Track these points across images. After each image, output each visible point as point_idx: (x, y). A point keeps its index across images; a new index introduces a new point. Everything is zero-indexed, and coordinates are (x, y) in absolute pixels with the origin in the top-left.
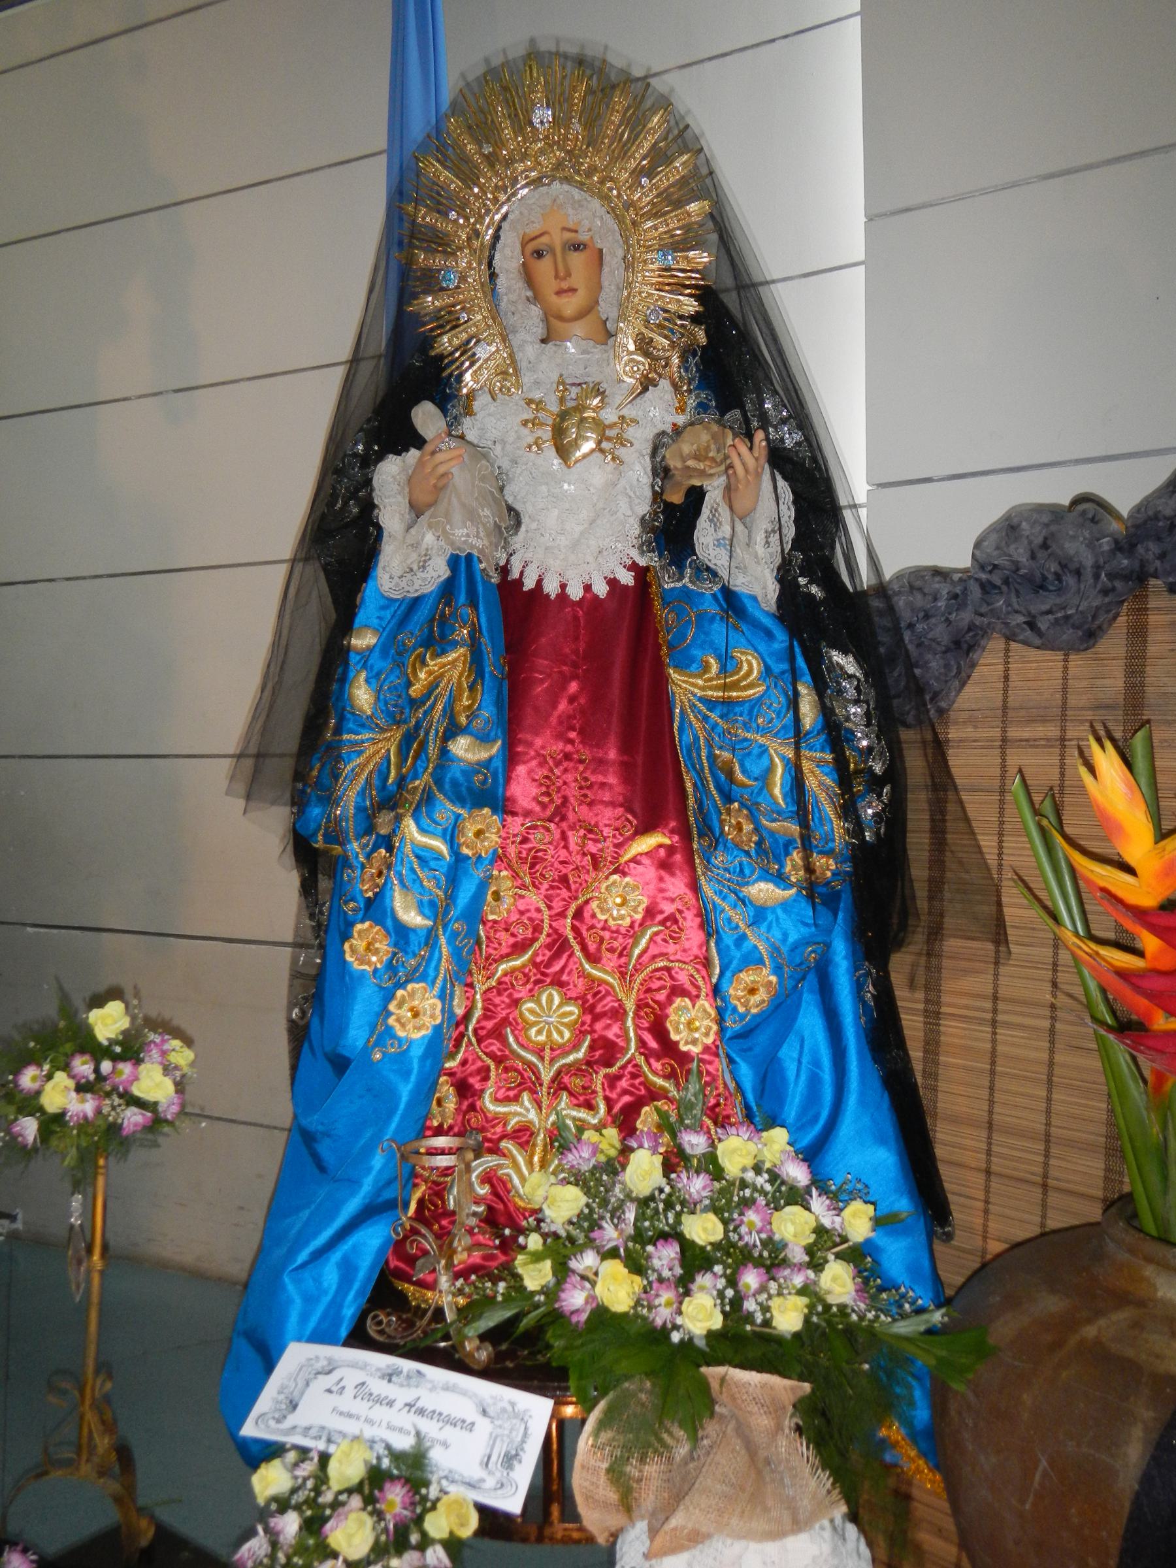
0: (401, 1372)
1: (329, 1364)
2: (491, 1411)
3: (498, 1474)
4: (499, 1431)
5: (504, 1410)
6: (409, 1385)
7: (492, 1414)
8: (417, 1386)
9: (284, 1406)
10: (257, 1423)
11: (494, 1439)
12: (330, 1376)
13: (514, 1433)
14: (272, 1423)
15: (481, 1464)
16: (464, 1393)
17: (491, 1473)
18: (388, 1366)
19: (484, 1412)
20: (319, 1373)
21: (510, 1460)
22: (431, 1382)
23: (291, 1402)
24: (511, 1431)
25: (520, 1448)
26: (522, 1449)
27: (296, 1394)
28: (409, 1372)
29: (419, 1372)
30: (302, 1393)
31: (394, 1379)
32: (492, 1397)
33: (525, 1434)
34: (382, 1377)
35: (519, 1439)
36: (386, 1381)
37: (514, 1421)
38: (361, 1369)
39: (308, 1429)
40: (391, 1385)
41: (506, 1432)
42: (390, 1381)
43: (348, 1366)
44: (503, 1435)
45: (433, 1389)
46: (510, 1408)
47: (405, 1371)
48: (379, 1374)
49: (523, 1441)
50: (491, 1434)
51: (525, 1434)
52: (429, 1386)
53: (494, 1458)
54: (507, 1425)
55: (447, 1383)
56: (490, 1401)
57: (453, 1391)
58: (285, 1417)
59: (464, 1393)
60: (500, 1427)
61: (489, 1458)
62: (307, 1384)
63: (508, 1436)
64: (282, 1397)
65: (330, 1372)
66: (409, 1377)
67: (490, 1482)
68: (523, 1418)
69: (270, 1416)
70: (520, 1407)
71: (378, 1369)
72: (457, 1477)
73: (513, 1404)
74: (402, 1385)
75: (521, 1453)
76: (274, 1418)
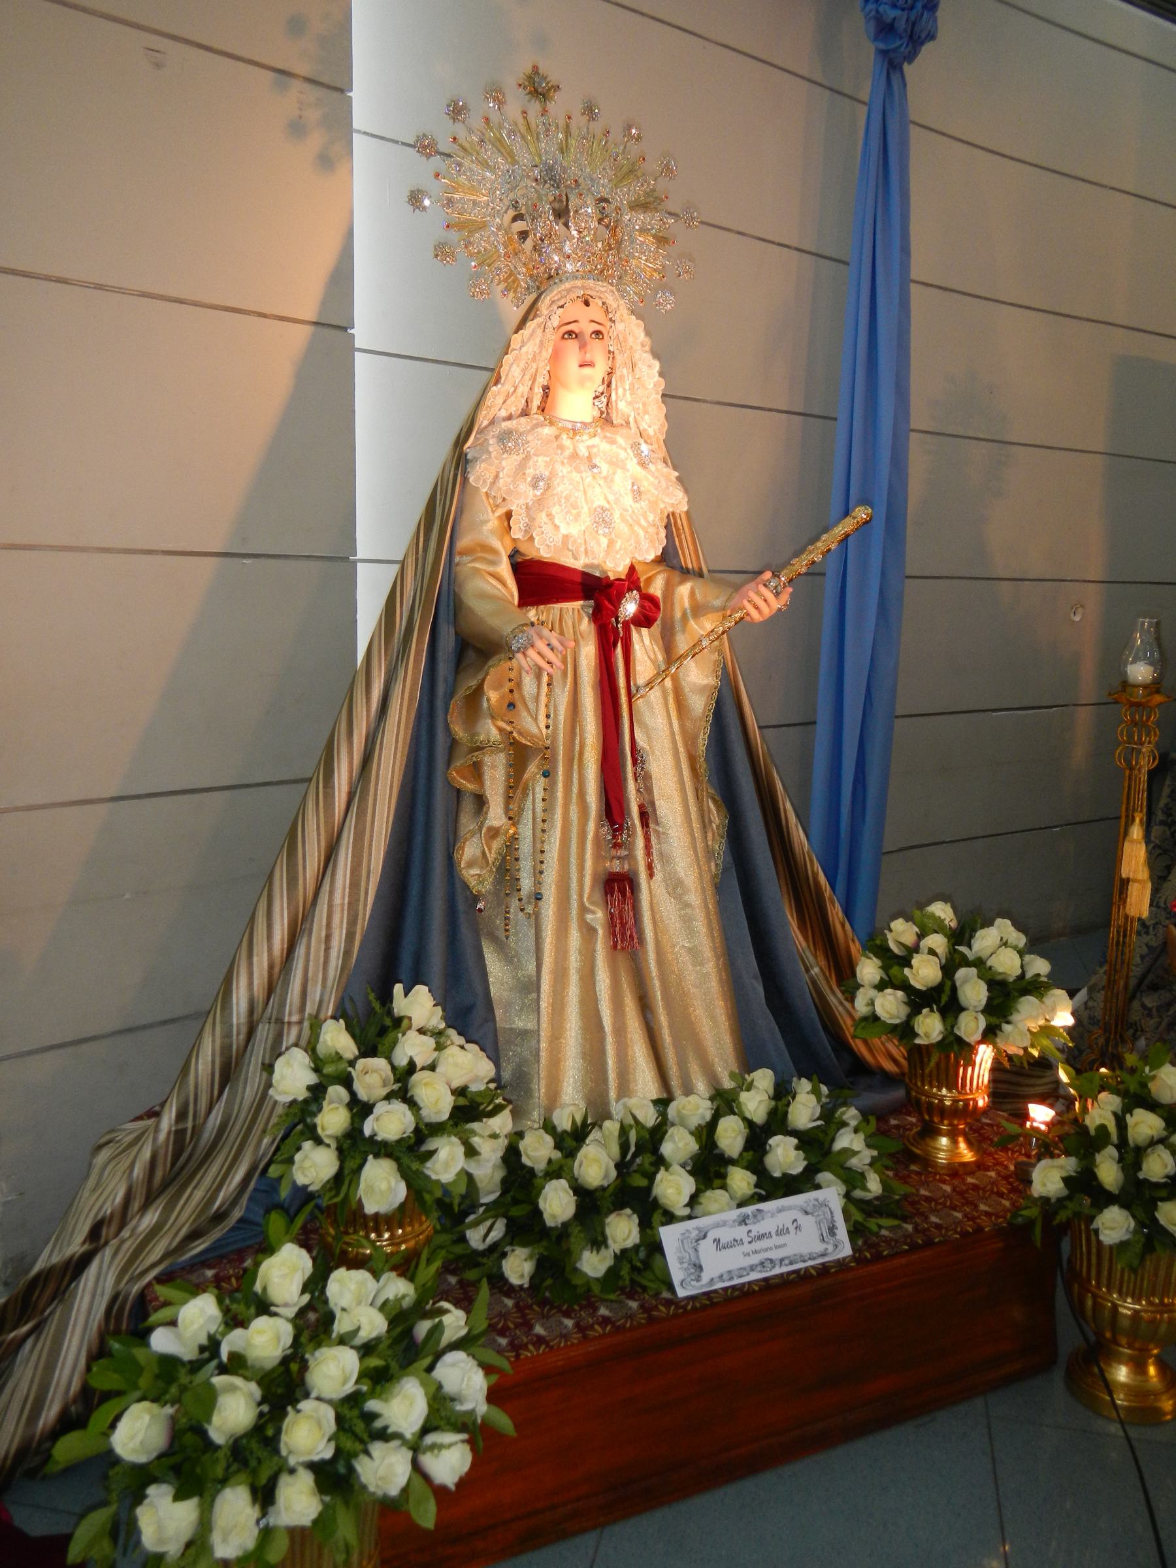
1: (700, 1231)
2: (809, 1209)
4: (819, 1218)
5: (814, 1205)
6: (758, 1221)
8: (763, 1219)
9: (693, 1271)
11: (819, 1223)
12: (707, 1239)
14: (694, 1283)
16: (790, 1208)
17: (828, 1243)
19: (807, 1213)
20: (697, 1240)
21: (832, 1230)
22: (769, 1212)
23: (695, 1265)
25: (833, 1221)
27: (693, 1259)
29: (758, 1210)
30: (698, 1257)
33: (831, 1213)
34: (740, 1224)
39: (721, 1277)
42: (746, 1224)
47: (750, 1213)
49: (832, 1217)
51: (831, 1213)
58: (699, 1276)
59: (790, 1208)
62: (696, 1250)
64: (685, 1265)
65: (705, 1237)
66: (755, 1216)
67: (830, 1248)
68: (824, 1204)
69: (689, 1279)
70: (821, 1199)
71: (734, 1221)
73: (817, 1200)
74: (755, 1223)
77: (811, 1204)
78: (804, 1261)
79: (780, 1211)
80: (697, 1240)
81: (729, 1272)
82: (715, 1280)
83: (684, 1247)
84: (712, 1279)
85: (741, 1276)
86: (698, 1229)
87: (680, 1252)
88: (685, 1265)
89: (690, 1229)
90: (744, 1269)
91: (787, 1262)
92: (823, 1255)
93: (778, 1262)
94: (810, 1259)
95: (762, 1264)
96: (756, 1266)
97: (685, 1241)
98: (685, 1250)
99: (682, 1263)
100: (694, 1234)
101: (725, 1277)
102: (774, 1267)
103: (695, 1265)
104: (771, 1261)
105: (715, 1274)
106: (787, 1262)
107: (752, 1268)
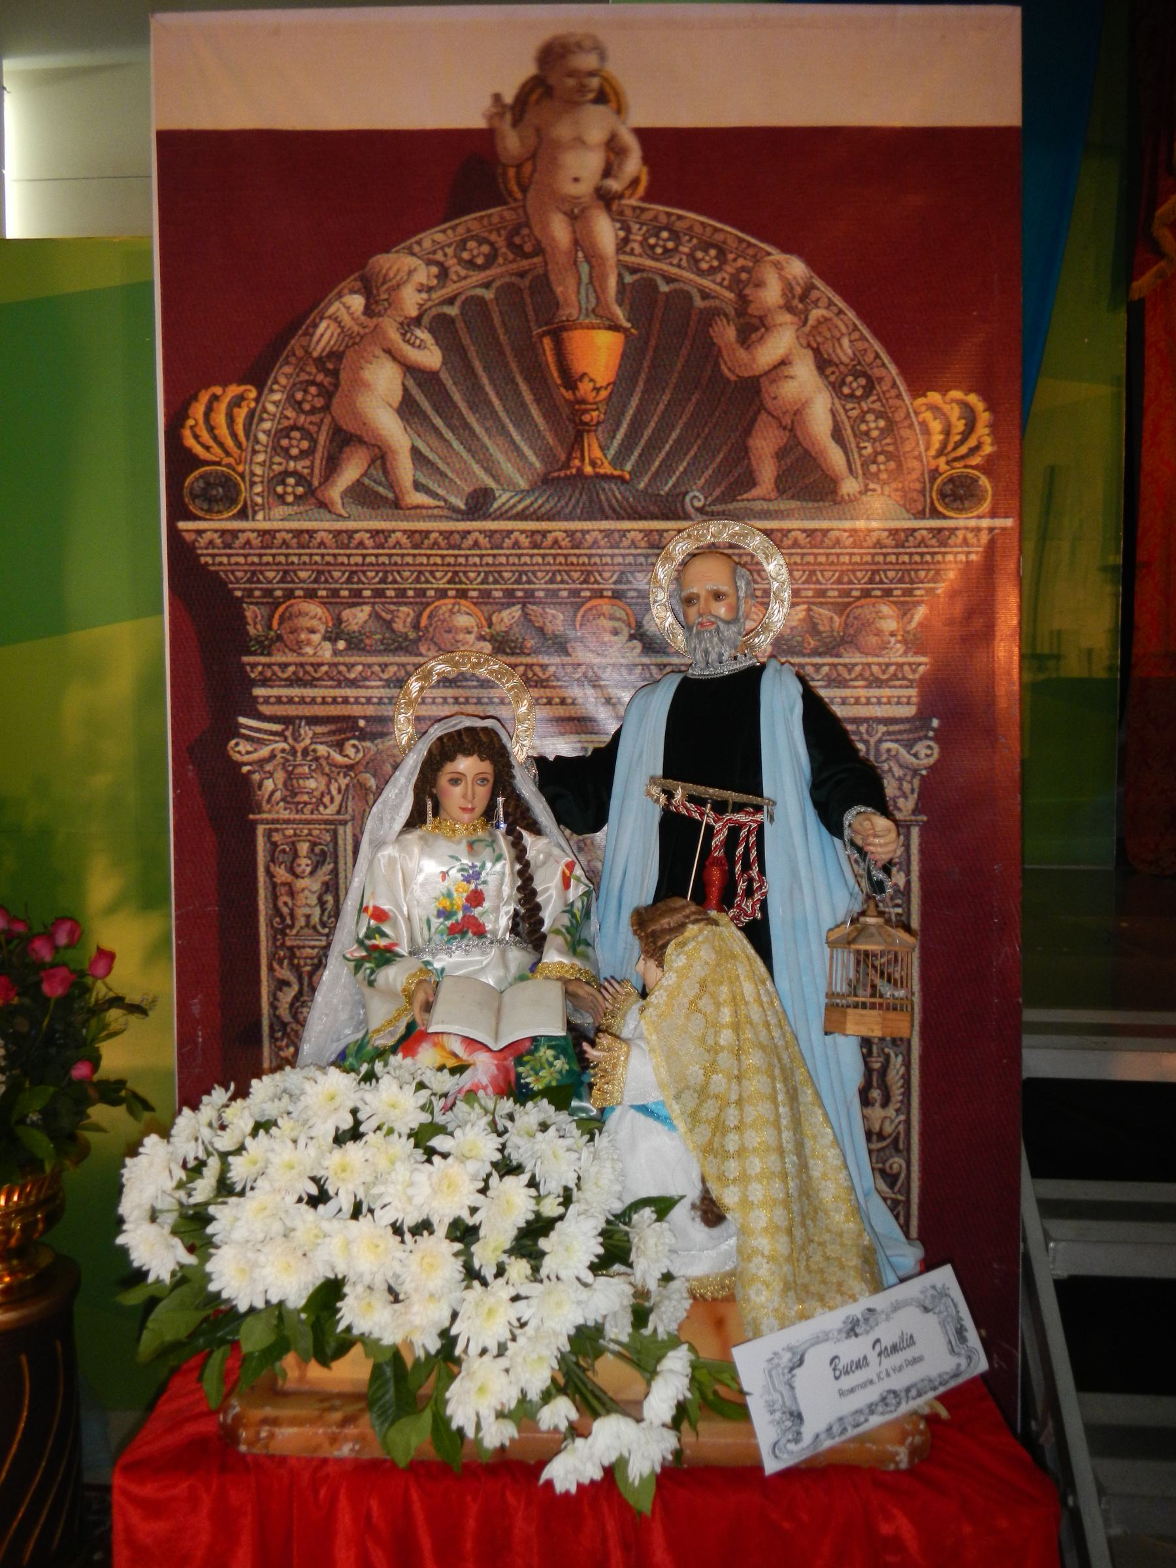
0: (858, 1320)
1: (794, 1354)
2: (928, 1304)
3: (963, 1352)
6: (872, 1328)
7: (930, 1307)
8: (877, 1324)
9: (789, 1424)
10: (776, 1457)
14: (791, 1447)
20: (792, 1369)
22: (883, 1312)
23: (791, 1414)
25: (960, 1319)
27: (788, 1403)
30: (794, 1399)
31: (858, 1330)
34: (848, 1336)
40: (860, 1338)
42: (856, 1335)
47: (860, 1316)
48: (844, 1335)
52: (883, 1316)
54: (942, 1308)
58: (799, 1433)
61: (950, 1342)
62: (792, 1388)
64: (778, 1415)
66: (866, 1320)
67: (964, 1362)
69: (783, 1441)
71: (840, 1331)
74: (867, 1332)
76: (789, 1441)
83: (773, 1383)
84: (817, 1436)
87: (769, 1393)
88: (778, 1415)
91: (913, 1393)
92: (956, 1375)
93: (903, 1394)
94: (941, 1384)
96: (877, 1405)
97: (774, 1373)
98: (775, 1389)
99: (772, 1412)
102: (899, 1404)
103: (791, 1414)
104: (895, 1393)
106: (913, 1393)
107: (871, 1409)
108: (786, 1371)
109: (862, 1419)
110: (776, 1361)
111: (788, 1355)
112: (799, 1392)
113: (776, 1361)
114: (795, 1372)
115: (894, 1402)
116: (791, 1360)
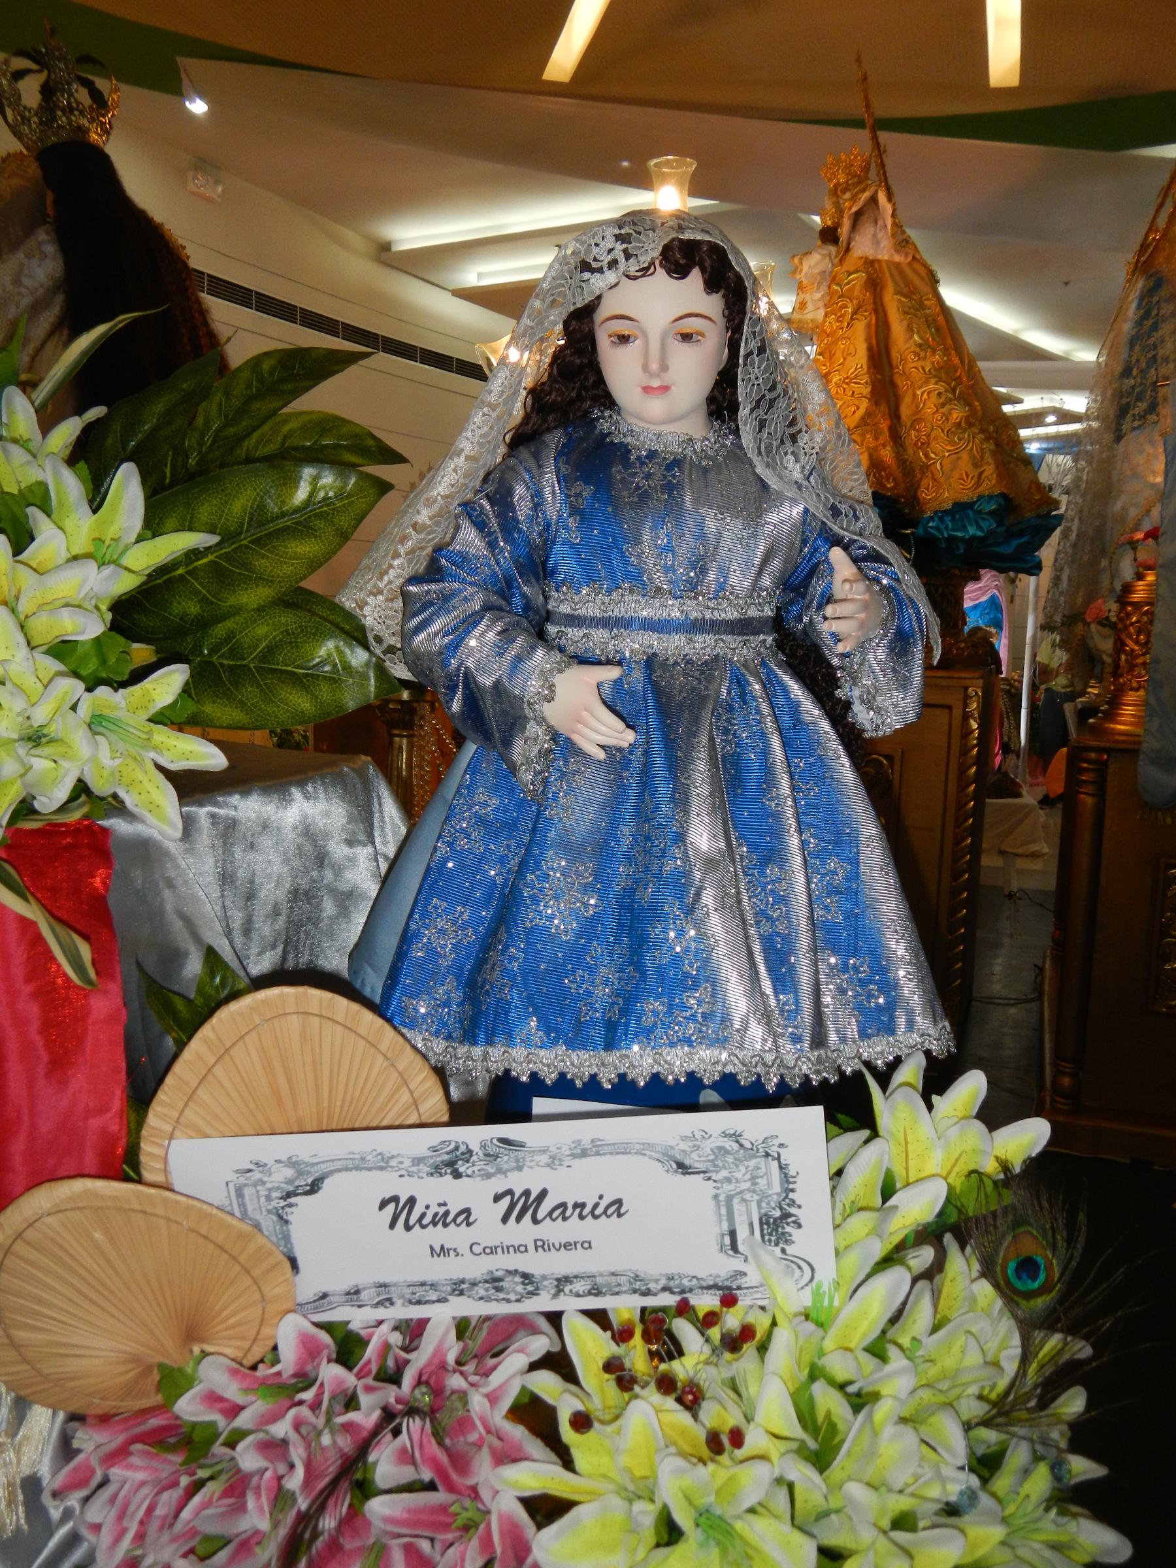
0: (470, 1152)
1: (300, 1173)
2: (692, 1160)
4: (728, 1188)
6: (499, 1171)
7: (701, 1166)
8: (520, 1168)
13: (762, 1182)
15: (721, 1250)
16: (623, 1149)
18: (434, 1149)
19: (683, 1168)
20: (289, 1195)
22: (544, 1151)
24: (753, 1179)
26: (793, 1203)
28: (483, 1146)
32: (684, 1138)
33: (786, 1178)
35: (777, 1187)
36: (449, 1177)
37: (752, 1163)
38: (381, 1168)
40: (464, 1179)
41: (746, 1185)
42: (457, 1175)
43: (347, 1169)
44: (742, 1192)
45: (554, 1162)
46: (732, 1145)
48: (426, 1169)
50: (716, 1197)
51: (786, 1178)
52: (544, 1159)
53: (742, 1234)
55: (578, 1142)
56: (684, 1146)
57: (597, 1154)
59: (623, 1149)
60: (728, 1180)
61: (733, 1234)
63: (754, 1191)
65: (314, 1188)
68: (769, 1152)
71: (418, 1161)
72: (686, 1282)
73: (736, 1137)
74: (488, 1176)
75: (793, 1210)
77: (708, 1146)
78: (647, 1293)
79: (584, 1154)
80: (289, 1195)
81: (384, 1285)
82: (332, 1299)
84: (325, 1296)
85: (419, 1302)
86: (292, 1163)
89: (270, 1162)
90: (433, 1286)
94: (665, 1289)
95: (495, 1281)
96: (474, 1284)
97: (247, 1192)
100: (281, 1176)
101: (364, 1295)
104: (525, 1276)
105: (338, 1284)
106: (579, 1286)
108: (275, 1194)
109: (433, 1296)
110: (257, 1175)
111: (289, 1173)
112: (293, 1229)
113: (257, 1175)
114: (293, 1200)
115: (520, 1288)
116: (289, 1182)
